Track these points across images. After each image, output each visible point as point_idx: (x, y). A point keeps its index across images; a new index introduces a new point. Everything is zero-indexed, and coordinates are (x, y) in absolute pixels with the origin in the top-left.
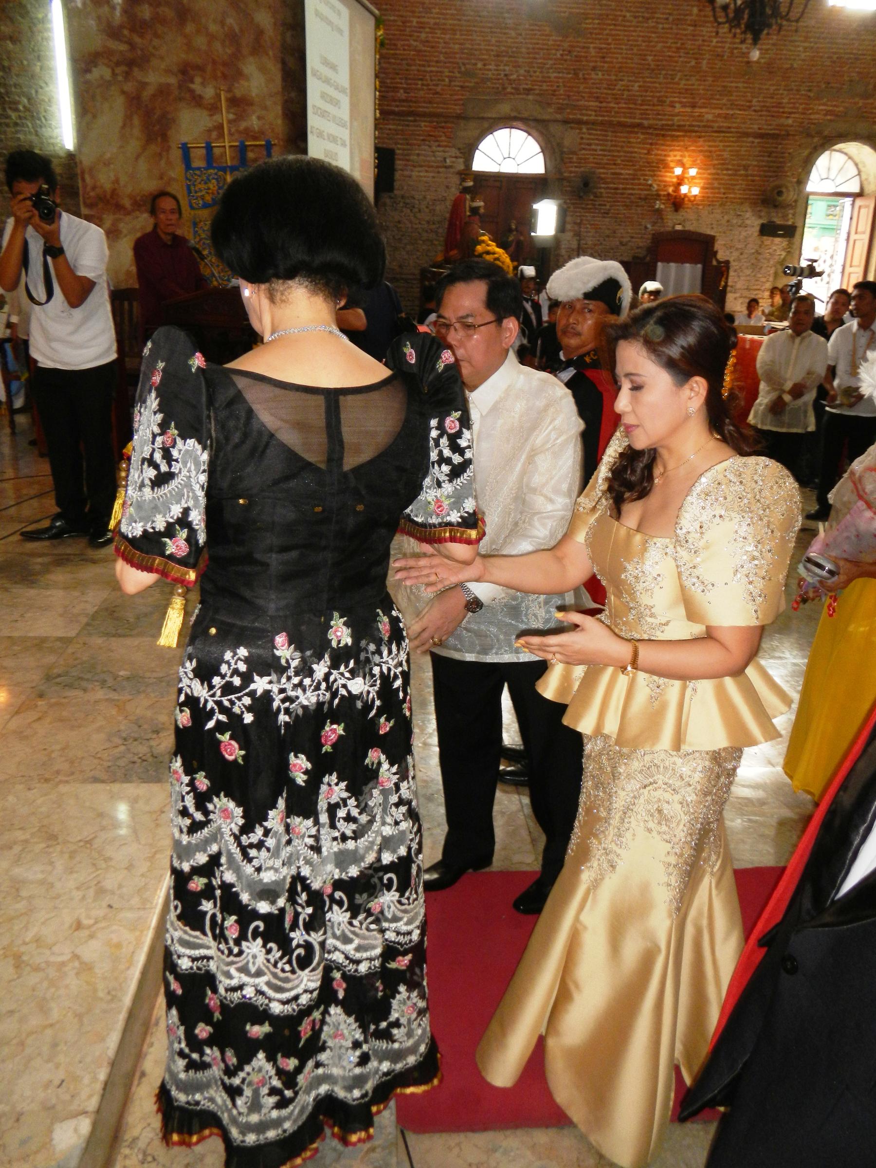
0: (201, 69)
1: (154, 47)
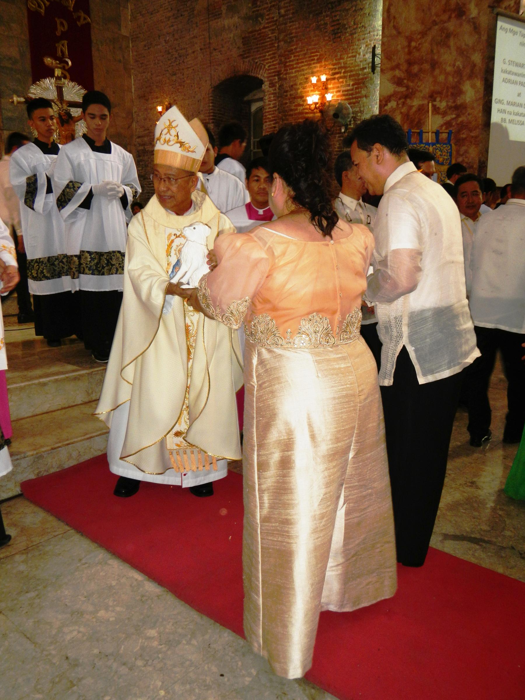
0: (440, 93)
1: (418, 87)
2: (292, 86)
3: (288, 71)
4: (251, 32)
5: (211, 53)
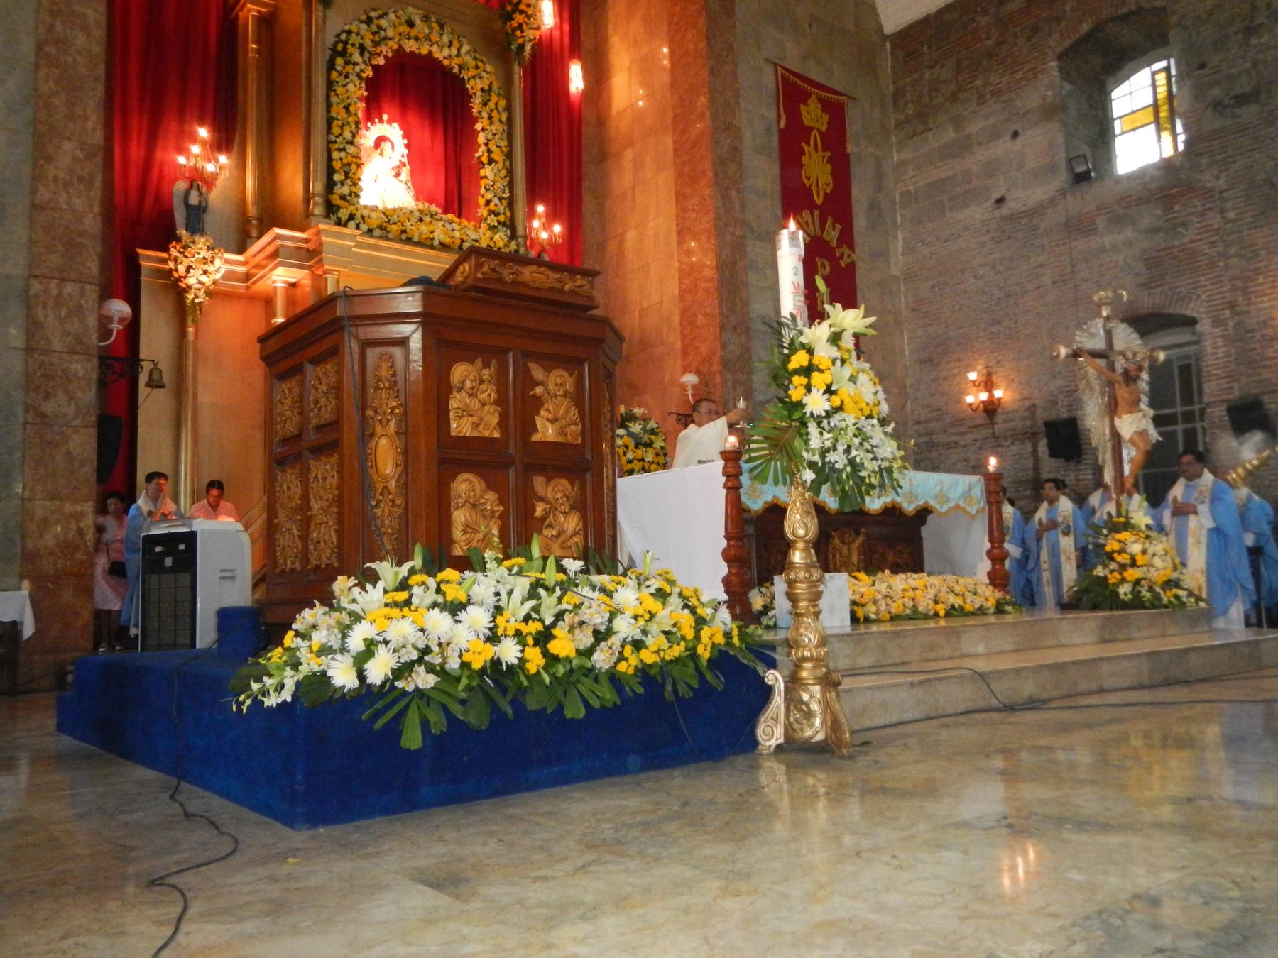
2: (1264, 322)
3: (1254, 300)
4: (1164, 249)
5: (1076, 286)
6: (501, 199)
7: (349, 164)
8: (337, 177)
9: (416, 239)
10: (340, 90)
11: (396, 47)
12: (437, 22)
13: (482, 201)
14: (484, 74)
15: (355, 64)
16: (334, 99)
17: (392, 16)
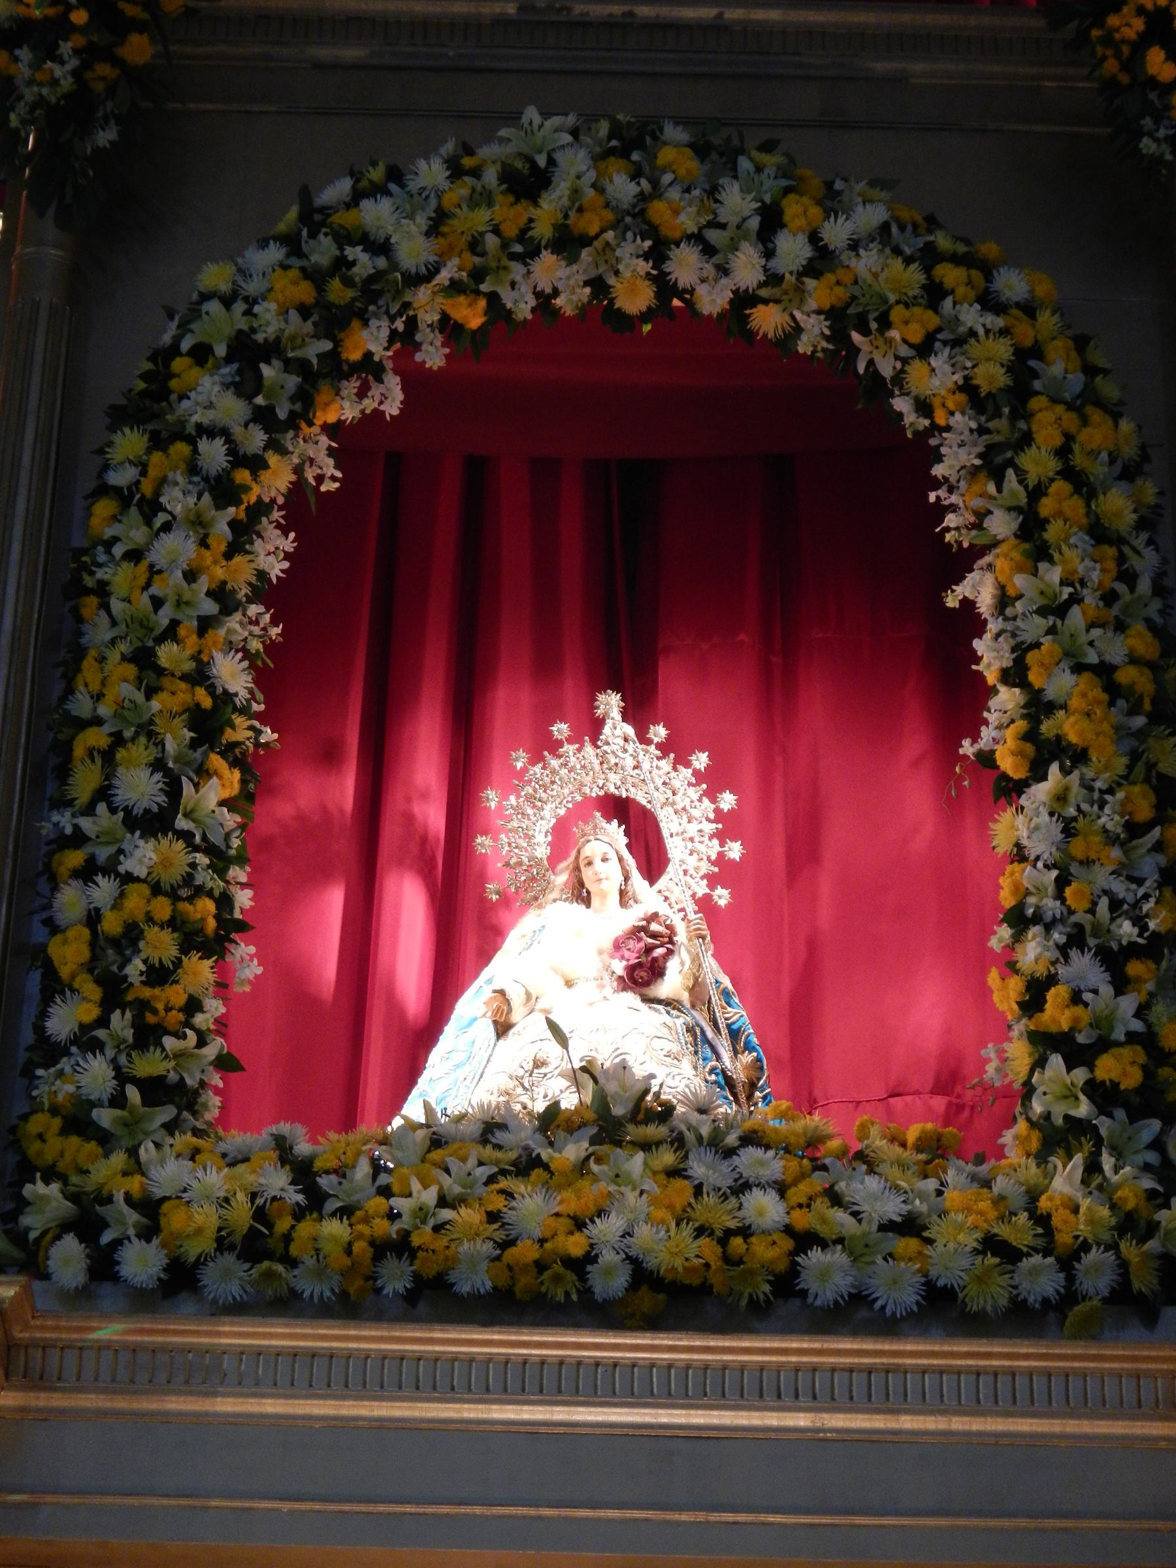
6: (1114, 961)
7: (132, 935)
8: (63, 1020)
9: (474, 1279)
10: (122, 577)
11: (472, 316)
12: (700, 150)
13: (1006, 994)
14: (971, 316)
15: (209, 432)
16: (99, 631)
17: (430, 173)
